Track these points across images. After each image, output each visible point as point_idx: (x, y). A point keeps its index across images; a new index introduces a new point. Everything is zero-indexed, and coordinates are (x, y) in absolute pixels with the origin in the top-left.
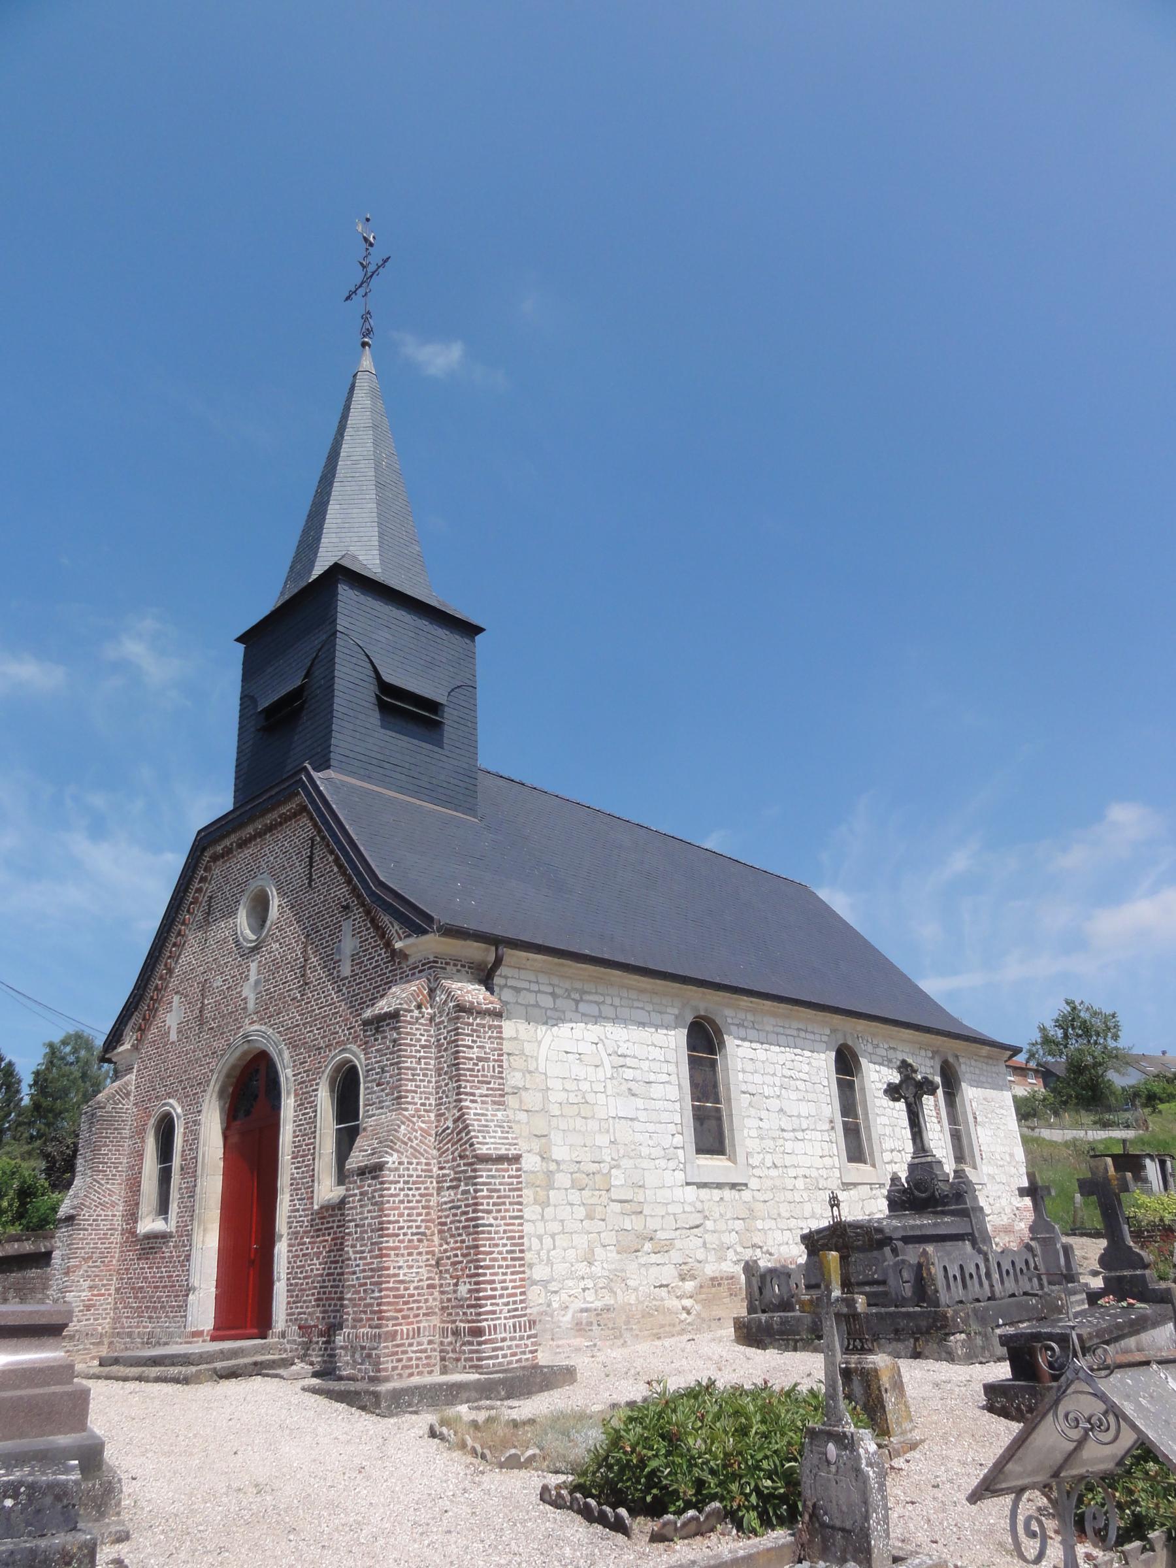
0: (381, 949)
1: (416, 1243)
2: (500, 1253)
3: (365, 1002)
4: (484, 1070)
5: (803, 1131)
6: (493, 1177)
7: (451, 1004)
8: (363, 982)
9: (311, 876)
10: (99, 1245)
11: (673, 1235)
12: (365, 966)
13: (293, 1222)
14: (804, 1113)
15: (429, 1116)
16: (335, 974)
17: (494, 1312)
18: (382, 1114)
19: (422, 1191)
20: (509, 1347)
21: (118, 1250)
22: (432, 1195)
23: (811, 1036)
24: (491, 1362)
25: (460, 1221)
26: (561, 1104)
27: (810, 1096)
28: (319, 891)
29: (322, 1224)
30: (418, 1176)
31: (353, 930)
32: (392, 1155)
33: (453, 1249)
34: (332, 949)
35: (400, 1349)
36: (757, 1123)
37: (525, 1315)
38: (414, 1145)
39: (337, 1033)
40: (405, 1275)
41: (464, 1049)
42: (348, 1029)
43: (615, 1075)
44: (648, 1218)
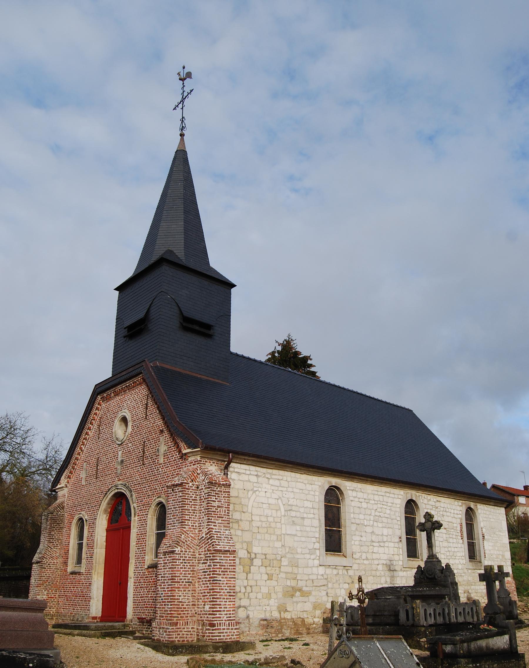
0: (177, 452)
1: (187, 586)
2: (224, 592)
3: (169, 476)
4: (220, 512)
5: (384, 542)
6: (222, 560)
7: (207, 481)
8: (169, 467)
9: (147, 413)
10: (51, 576)
11: (311, 589)
12: (170, 459)
13: (136, 573)
14: (385, 533)
15: (195, 531)
16: (156, 462)
17: (220, 617)
18: (174, 529)
19: (191, 564)
20: (226, 633)
21: (59, 579)
22: (195, 566)
23: (392, 495)
24: (218, 638)
25: (207, 578)
26: (258, 527)
27: (390, 525)
28: (150, 421)
29: (149, 574)
30: (189, 557)
31: (165, 442)
32: (178, 548)
33: (203, 590)
34: (155, 450)
35: (179, 630)
36: (358, 538)
37: (234, 620)
38: (188, 543)
39: (157, 489)
40: (182, 599)
41: (211, 502)
42: (162, 488)
43: (286, 515)
44: (299, 581)
